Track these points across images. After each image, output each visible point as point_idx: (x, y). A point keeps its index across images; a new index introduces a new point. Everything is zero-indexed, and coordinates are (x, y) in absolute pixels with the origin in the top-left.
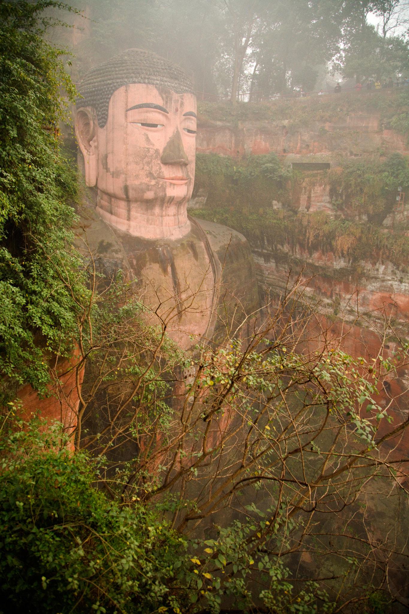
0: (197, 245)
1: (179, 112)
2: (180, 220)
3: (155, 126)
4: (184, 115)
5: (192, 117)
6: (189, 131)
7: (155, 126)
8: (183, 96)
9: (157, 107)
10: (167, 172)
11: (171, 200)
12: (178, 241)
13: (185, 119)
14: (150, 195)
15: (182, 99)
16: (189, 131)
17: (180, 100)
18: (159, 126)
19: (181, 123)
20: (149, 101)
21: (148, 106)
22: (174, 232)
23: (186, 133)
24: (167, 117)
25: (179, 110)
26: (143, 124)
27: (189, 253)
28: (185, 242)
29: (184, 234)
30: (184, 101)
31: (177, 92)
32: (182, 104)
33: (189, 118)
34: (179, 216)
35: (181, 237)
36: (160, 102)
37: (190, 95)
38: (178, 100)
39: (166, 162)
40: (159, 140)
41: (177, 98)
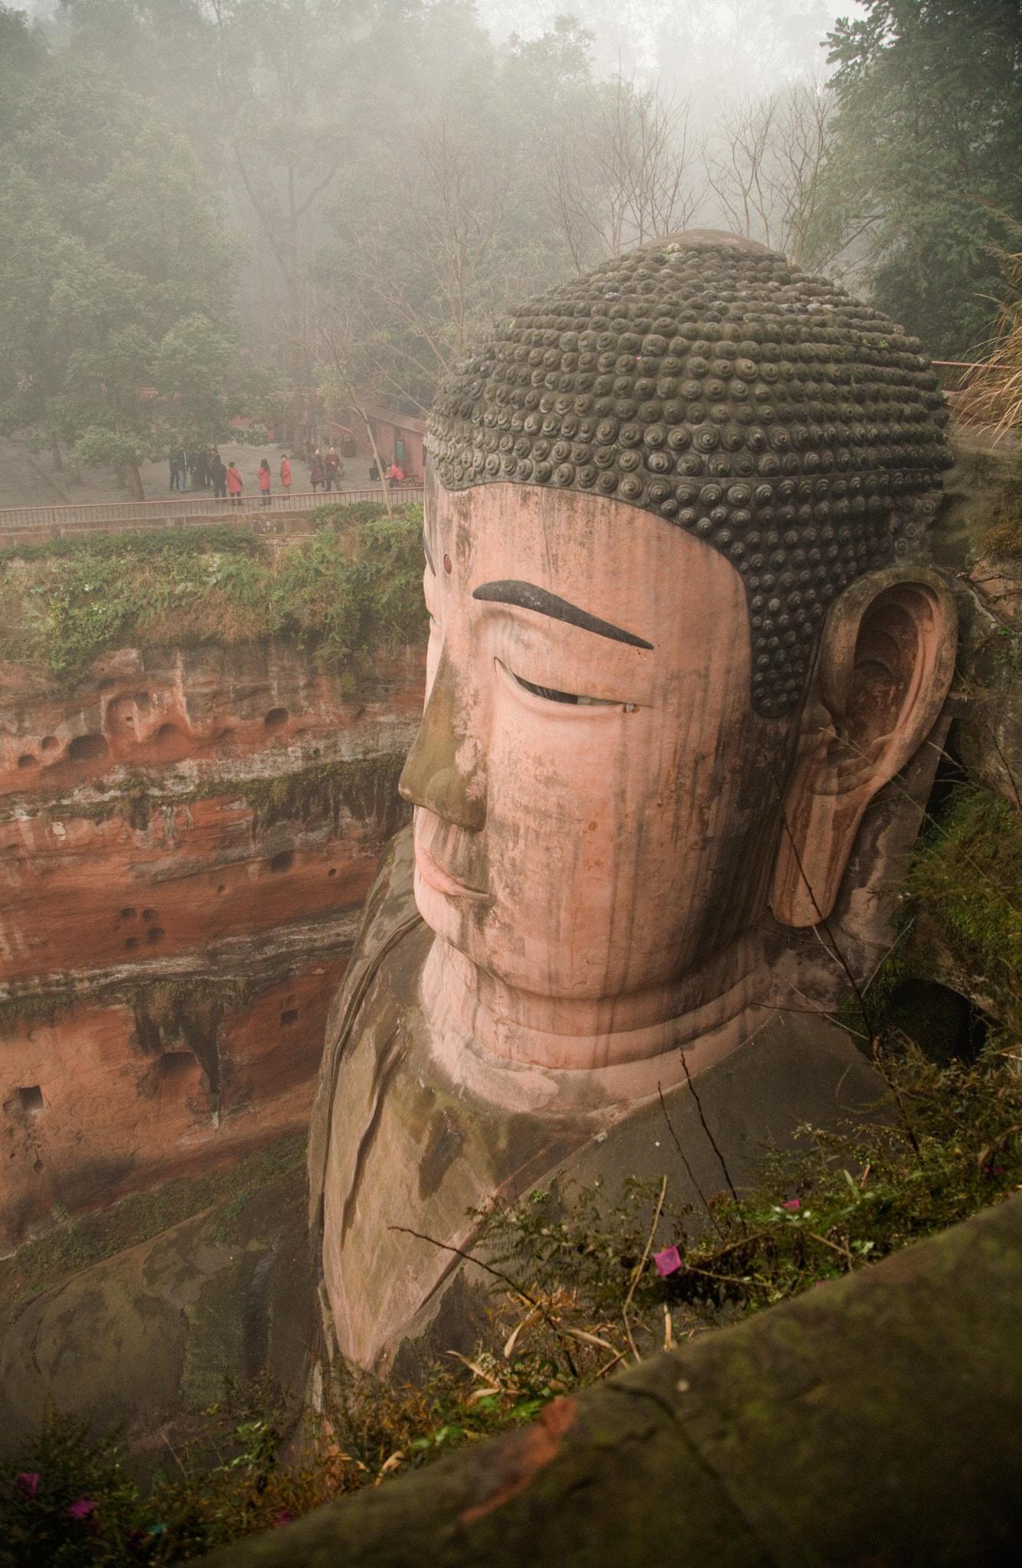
0: (461, 1165)
1: (454, 575)
2: (478, 1024)
5: (516, 610)
8: (470, 498)
12: (436, 1073)
13: (494, 614)
15: (465, 516)
17: (456, 518)
19: (475, 630)
22: (448, 1036)
25: (455, 567)
27: (418, 1141)
28: (441, 1101)
29: (470, 1083)
30: (474, 524)
31: (449, 484)
32: (465, 539)
33: (512, 617)
34: (480, 1011)
35: (456, 1079)
37: (510, 493)
38: (450, 521)
41: (445, 512)
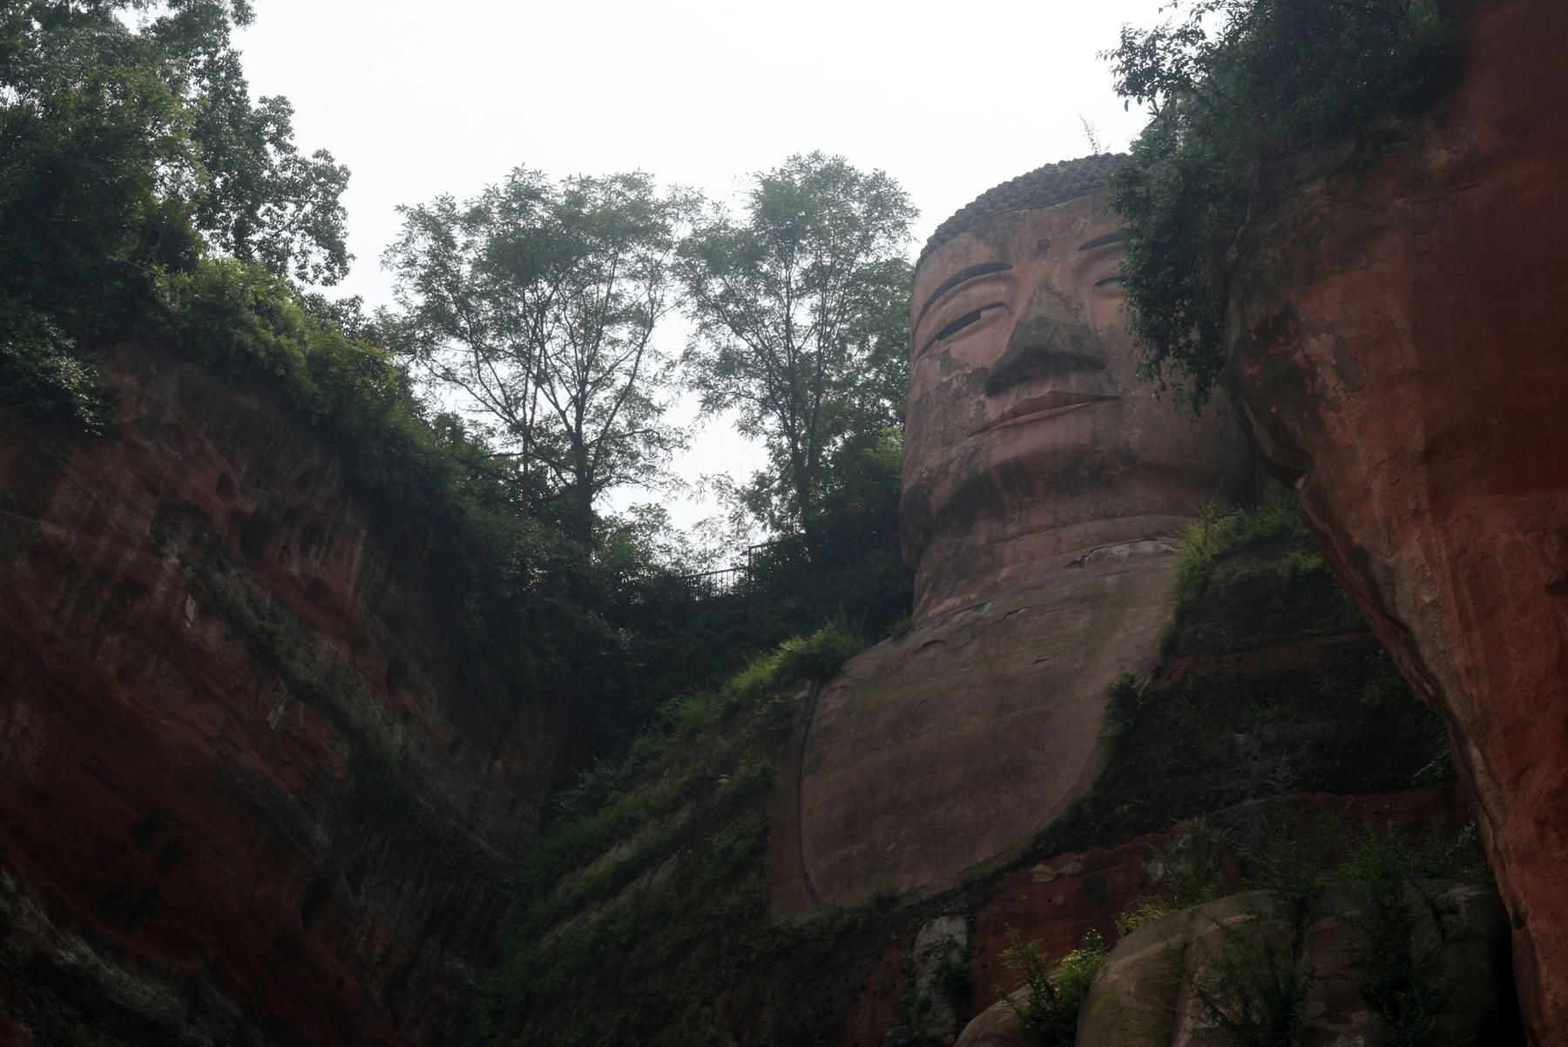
4: (1081, 249)
7: (973, 316)
14: (943, 493)
18: (984, 314)
20: (949, 274)
21: (949, 284)
24: (1006, 279)
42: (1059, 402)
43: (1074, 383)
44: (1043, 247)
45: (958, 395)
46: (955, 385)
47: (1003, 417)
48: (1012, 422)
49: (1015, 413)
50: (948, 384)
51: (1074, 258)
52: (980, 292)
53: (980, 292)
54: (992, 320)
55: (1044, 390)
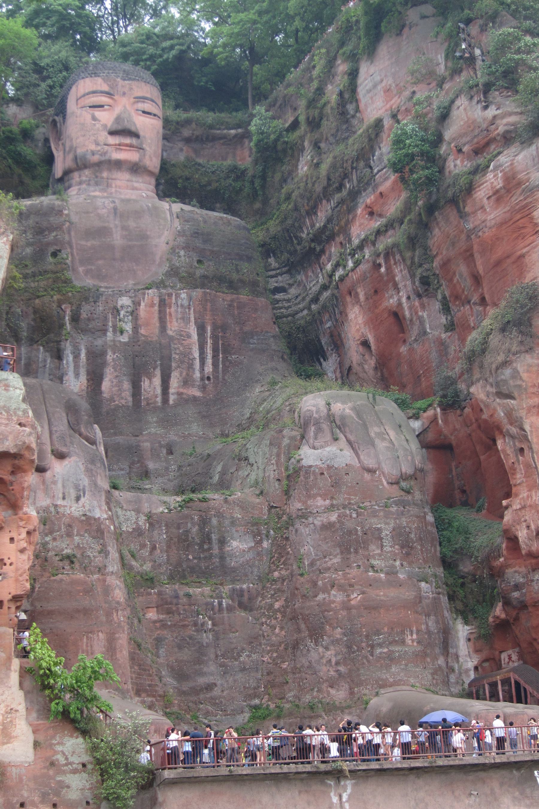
3: (102, 106)
6: (144, 112)
7: (102, 106)
9: (102, 92)
10: (113, 140)
11: (118, 164)
13: (138, 102)
14: (96, 158)
16: (144, 112)
21: (94, 92)
23: (141, 113)
24: (112, 99)
26: (90, 107)
32: (131, 89)
36: (105, 88)
39: (112, 133)
40: (106, 118)
42: (131, 146)
43: (134, 141)
44: (124, 94)
45: (98, 130)
46: (97, 126)
47: (116, 145)
48: (119, 147)
49: (119, 145)
50: (95, 125)
51: (132, 100)
52: (104, 100)
53: (104, 100)
54: (109, 110)
55: (128, 141)
